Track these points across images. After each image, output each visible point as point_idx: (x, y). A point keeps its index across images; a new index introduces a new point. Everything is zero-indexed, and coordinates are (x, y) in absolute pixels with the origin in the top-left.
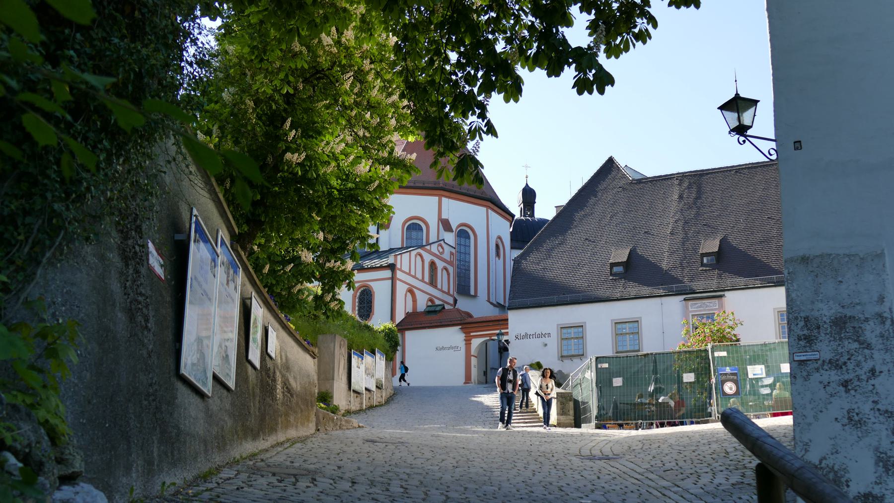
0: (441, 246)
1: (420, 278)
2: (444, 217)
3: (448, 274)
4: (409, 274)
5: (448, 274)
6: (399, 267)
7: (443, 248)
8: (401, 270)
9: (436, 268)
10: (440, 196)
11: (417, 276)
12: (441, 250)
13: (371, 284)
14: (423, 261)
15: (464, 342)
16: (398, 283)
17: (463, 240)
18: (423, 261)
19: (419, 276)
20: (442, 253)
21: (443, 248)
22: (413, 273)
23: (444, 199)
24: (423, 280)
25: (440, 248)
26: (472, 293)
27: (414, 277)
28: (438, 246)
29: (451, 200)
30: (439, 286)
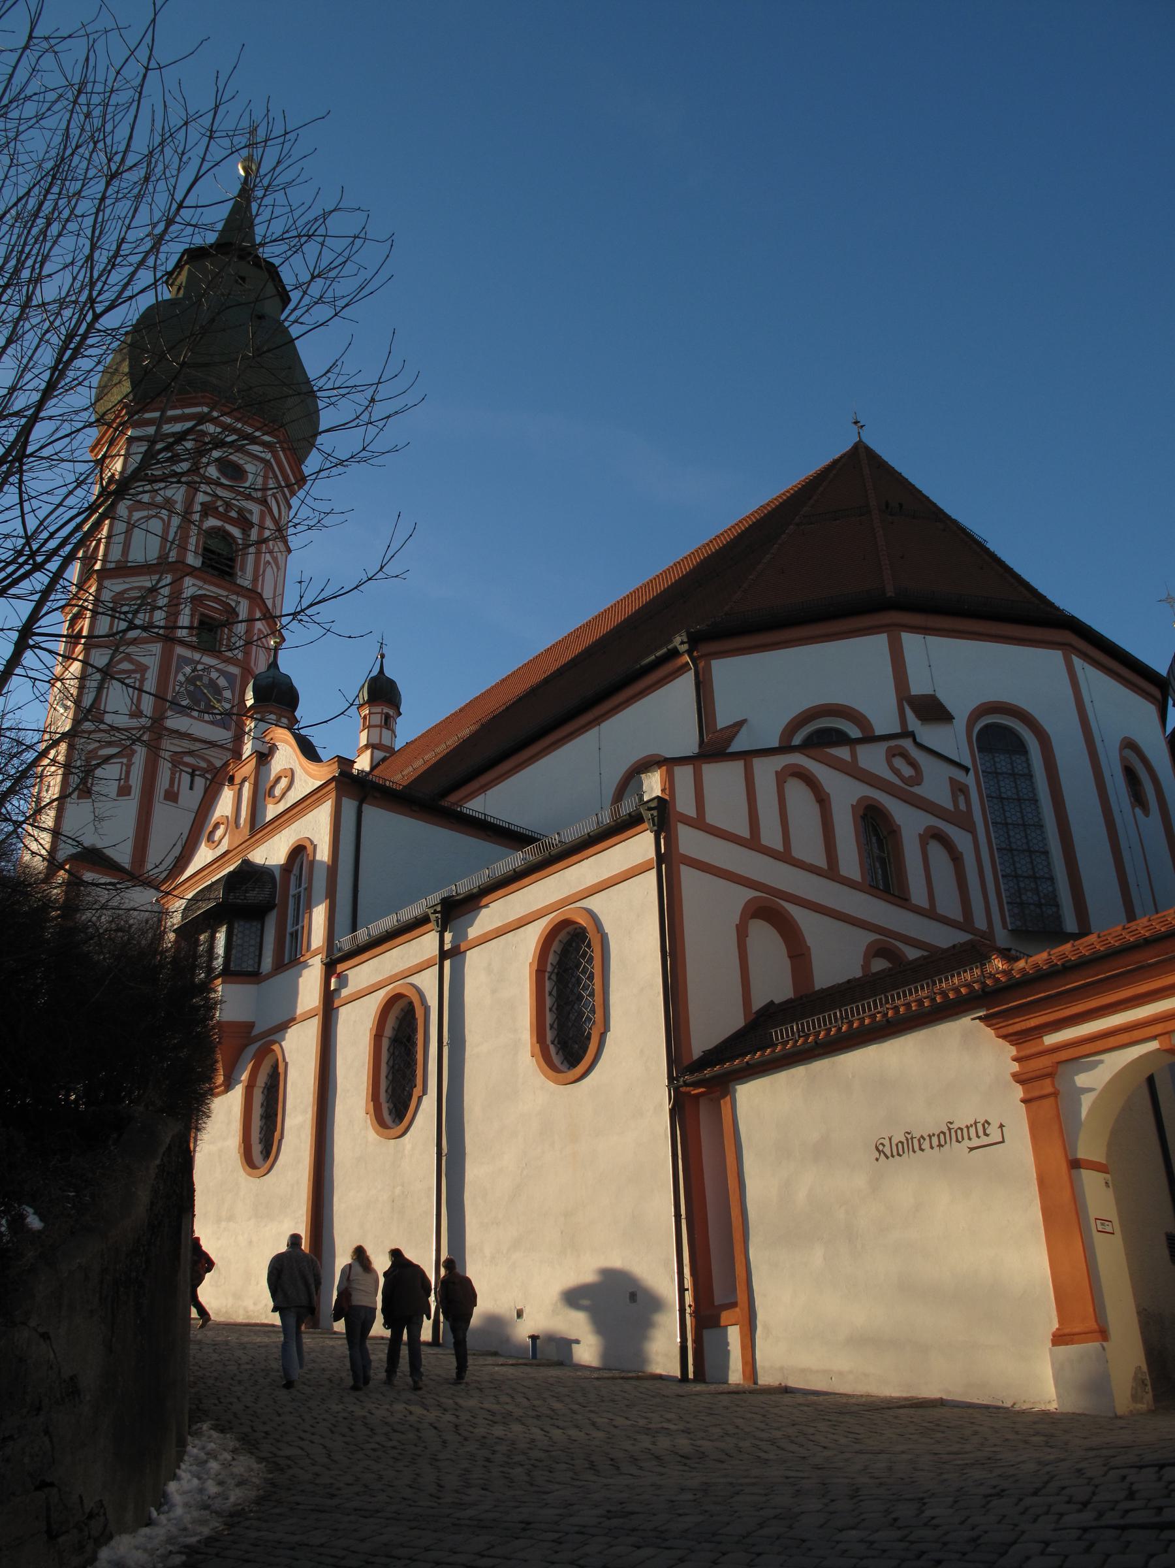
0: (904, 755)
1: (821, 862)
2: (918, 687)
3: (956, 858)
4: (753, 843)
5: (956, 858)
6: (691, 812)
7: (913, 764)
8: (699, 823)
9: (894, 832)
10: (893, 631)
11: (798, 853)
12: (908, 771)
13: (593, 903)
14: (822, 800)
15: (1019, 1092)
16: (687, 874)
17: (1002, 762)
18: (822, 800)
19: (810, 848)
20: (918, 779)
21: (913, 764)
22: (771, 836)
23: (911, 642)
24: (831, 872)
25: (899, 762)
26: (1071, 925)
27: (785, 857)
28: (891, 754)
29: (933, 641)
30: (918, 894)
